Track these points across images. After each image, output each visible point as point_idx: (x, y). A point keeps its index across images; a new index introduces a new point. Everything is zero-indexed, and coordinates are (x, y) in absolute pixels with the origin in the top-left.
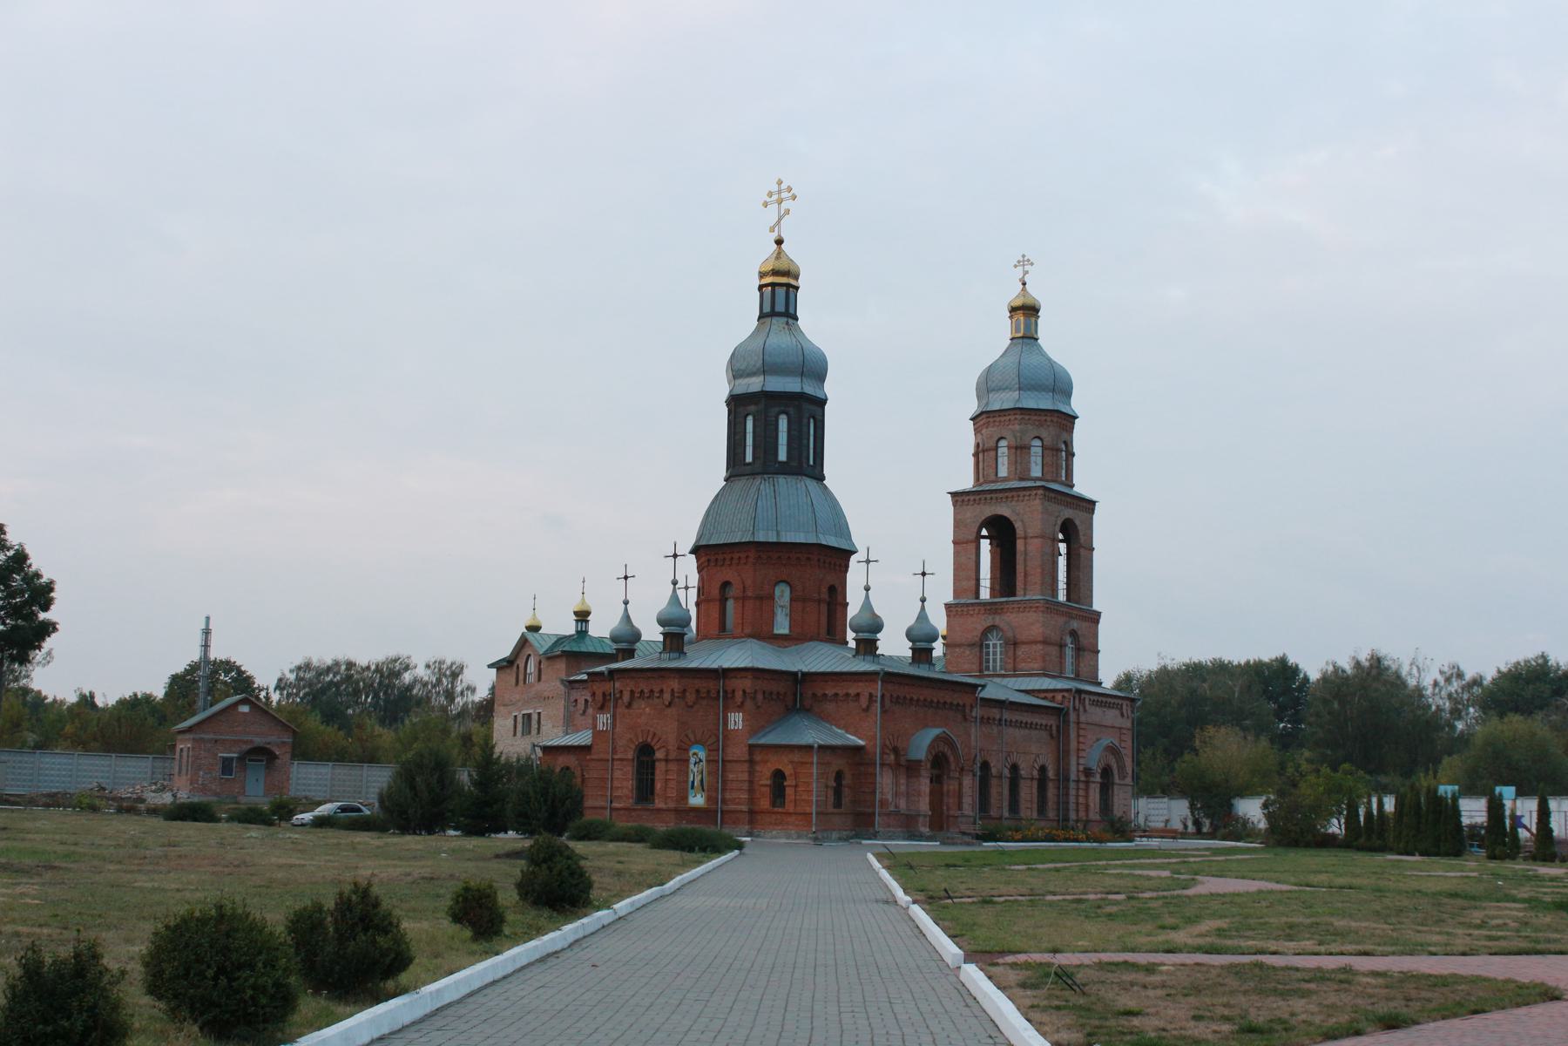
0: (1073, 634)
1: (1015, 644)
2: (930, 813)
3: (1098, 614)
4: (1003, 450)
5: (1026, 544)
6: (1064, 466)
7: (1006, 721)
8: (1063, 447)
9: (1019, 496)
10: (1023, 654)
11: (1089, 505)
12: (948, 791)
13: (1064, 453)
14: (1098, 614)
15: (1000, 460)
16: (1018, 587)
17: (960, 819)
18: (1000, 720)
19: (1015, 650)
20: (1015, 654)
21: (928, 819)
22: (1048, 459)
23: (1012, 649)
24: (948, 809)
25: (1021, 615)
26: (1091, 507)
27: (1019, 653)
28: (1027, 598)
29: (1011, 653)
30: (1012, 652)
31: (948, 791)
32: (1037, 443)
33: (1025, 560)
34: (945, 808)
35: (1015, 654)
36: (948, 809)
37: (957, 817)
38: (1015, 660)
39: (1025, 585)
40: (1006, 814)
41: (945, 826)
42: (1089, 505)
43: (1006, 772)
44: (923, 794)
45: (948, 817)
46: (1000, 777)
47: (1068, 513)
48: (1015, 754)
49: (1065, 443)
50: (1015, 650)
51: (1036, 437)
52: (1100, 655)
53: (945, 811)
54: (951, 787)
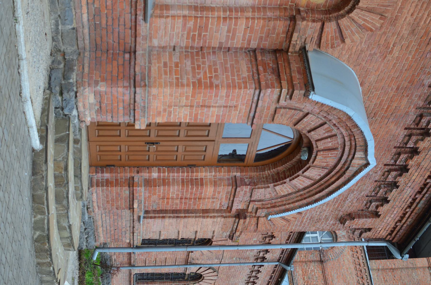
1: (321, 262)
2: (140, 125)
5: (424, 268)
7: (261, 266)
10: (312, 271)
12: (201, 183)
16: (379, 261)
17: (127, 213)
18: (263, 259)
19: (314, 261)
20: (311, 262)
21: (122, 119)
23: (315, 259)
24: (148, 183)
25: (352, 266)
27: (312, 266)
29: (311, 257)
30: (312, 259)
31: (201, 183)
33: (407, 268)
34: (155, 175)
35: (311, 262)
36: (148, 183)
37: (131, 208)
38: (305, 262)
39: (383, 270)
40: (136, 271)
41: (107, 175)
43: (192, 269)
44: (200, 98)
45: (131, 183)
46: (187, 262)
48: (215, 278)
50: (314, 261)
53: (145, 175)
54: (209, 190)
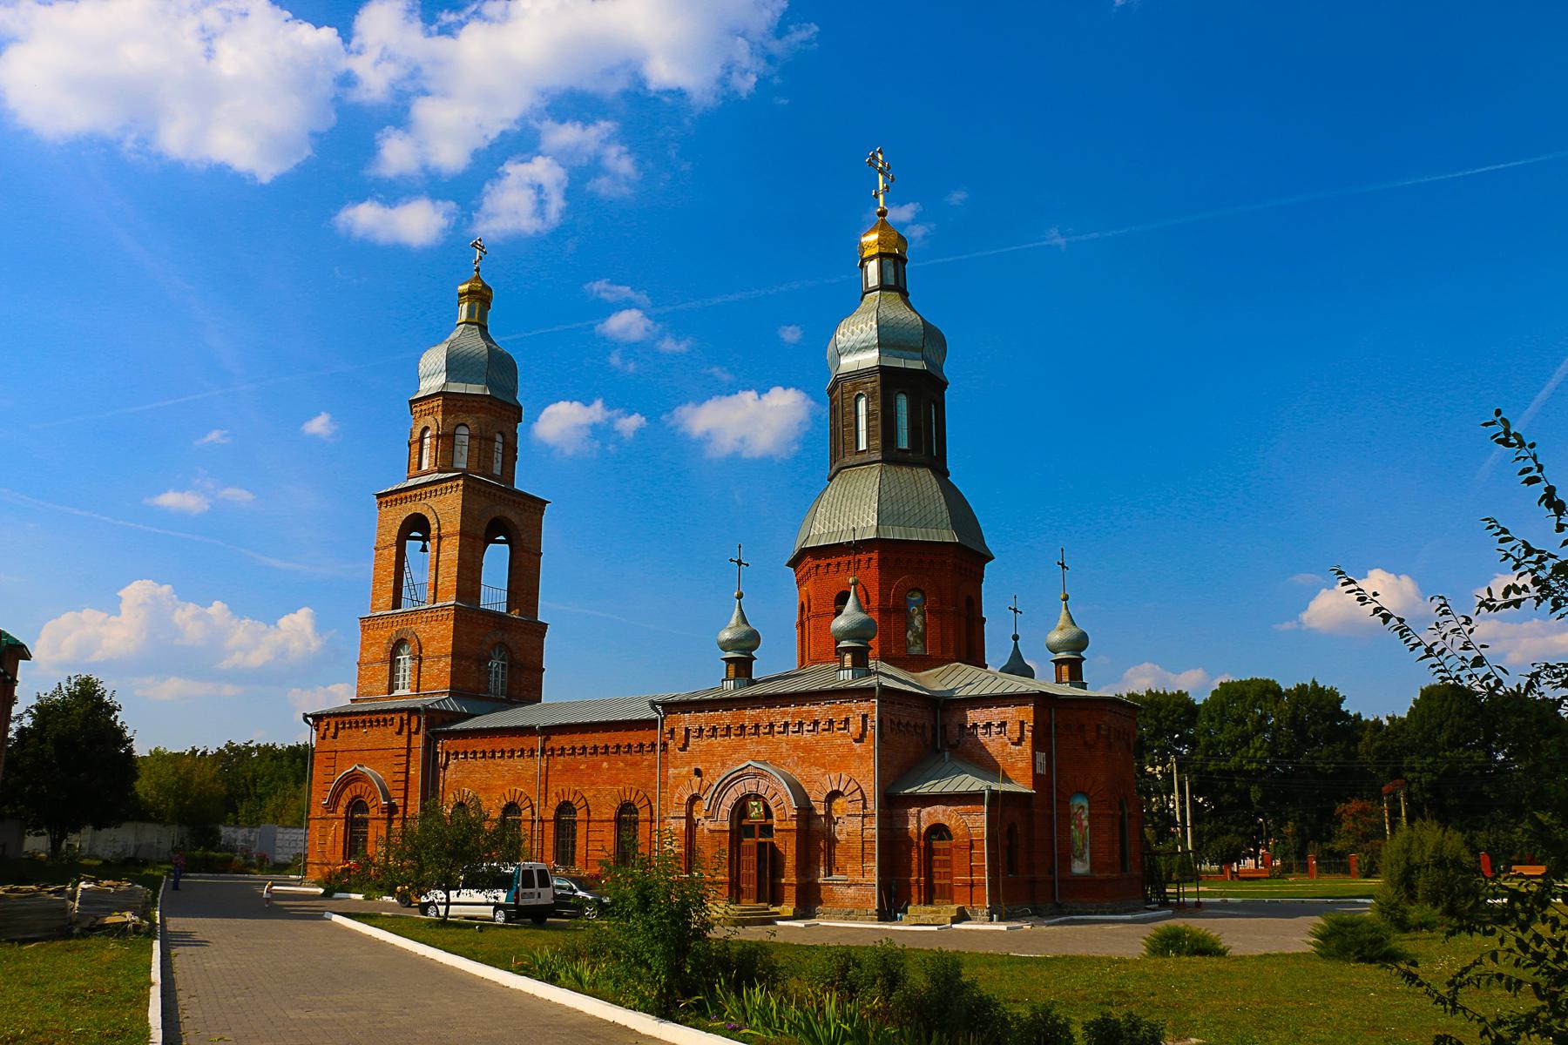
0: (503, 646)
3: (545, 626)
4: (427, 441)
6: (500, 460)
8: (499, 438)
9: (436, 490)
11: (537, 506)
13: (498, 446)
14: (545, 626)
15: (425, 451)
22: (476, 451)
26: (540, 506)
28: (438, 604)
32: (464, 431)
42: (537, 506)
47: (500, 511)
49: (499, 432)
51: (456, 428)
52: (544, 673)
